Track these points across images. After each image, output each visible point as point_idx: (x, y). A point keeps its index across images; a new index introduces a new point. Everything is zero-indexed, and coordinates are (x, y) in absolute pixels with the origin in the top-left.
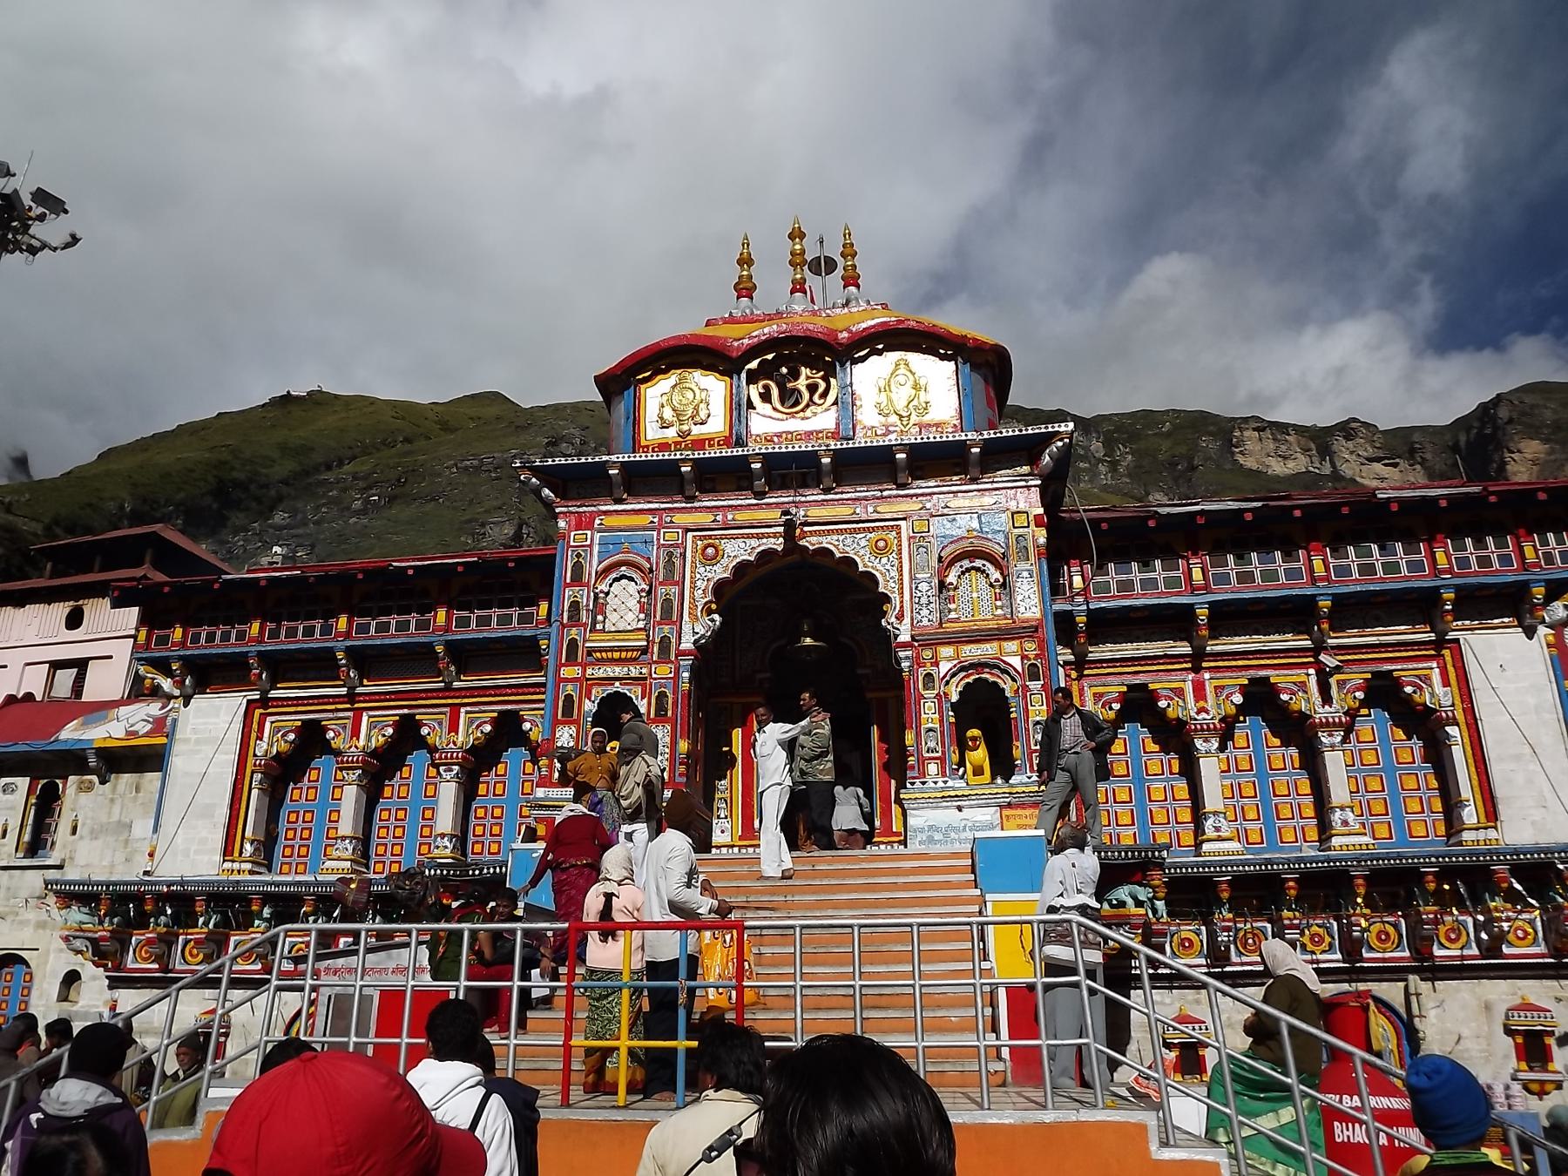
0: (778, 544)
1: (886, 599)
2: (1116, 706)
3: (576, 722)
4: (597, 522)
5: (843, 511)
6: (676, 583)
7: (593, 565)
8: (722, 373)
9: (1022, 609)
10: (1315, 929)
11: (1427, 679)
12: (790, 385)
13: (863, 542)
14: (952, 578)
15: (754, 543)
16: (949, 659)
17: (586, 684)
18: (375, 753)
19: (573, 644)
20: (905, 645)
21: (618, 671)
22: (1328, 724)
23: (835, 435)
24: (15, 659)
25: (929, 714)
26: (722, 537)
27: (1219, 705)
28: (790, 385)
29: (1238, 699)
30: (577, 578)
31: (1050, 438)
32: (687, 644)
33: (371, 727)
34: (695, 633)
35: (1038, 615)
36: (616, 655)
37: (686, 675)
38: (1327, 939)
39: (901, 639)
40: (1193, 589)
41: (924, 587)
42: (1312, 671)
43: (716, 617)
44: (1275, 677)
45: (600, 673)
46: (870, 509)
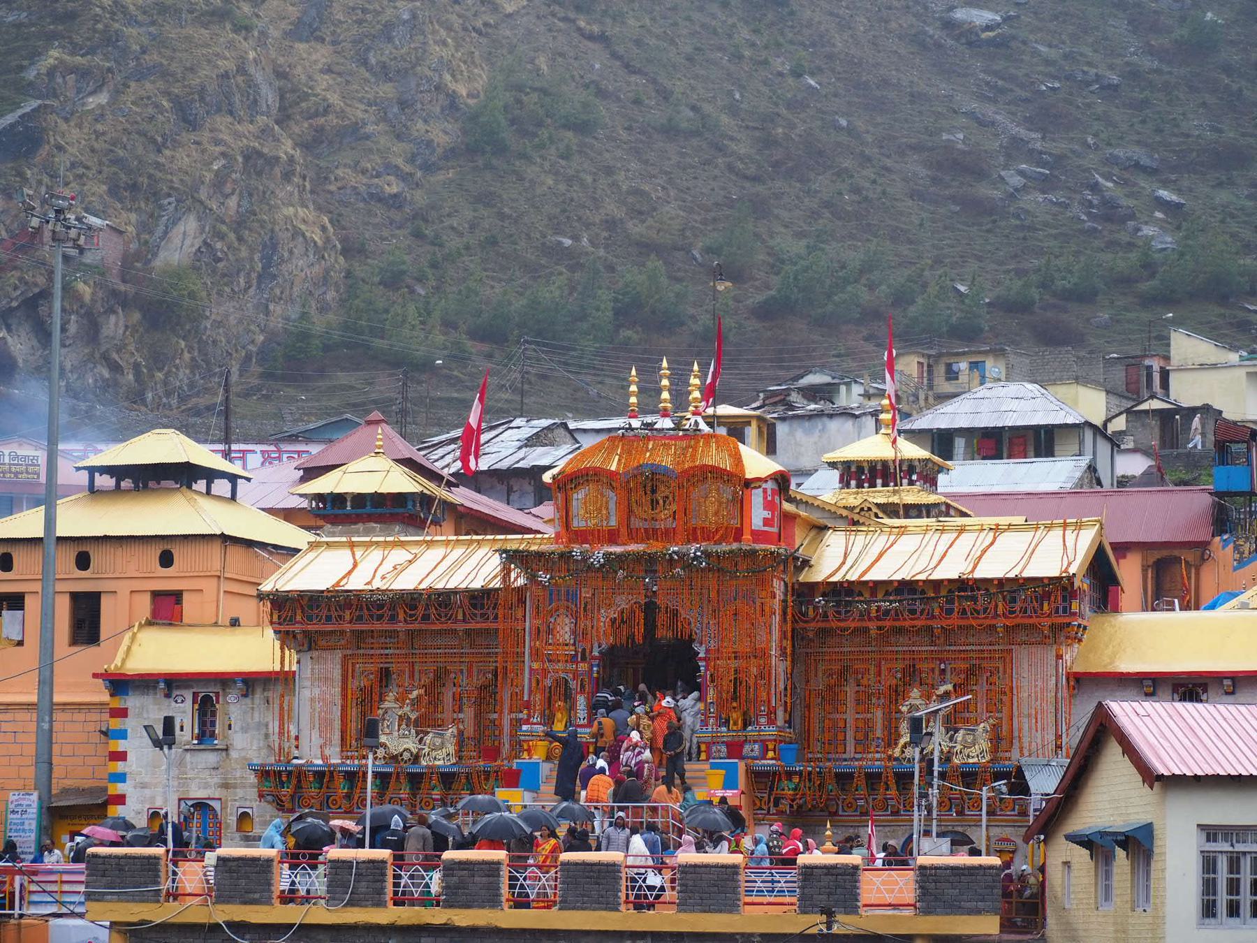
17: (545, 672)
20: (701, 659)
24: (124, 588)
32: (596, 653)
40: (870, 619)
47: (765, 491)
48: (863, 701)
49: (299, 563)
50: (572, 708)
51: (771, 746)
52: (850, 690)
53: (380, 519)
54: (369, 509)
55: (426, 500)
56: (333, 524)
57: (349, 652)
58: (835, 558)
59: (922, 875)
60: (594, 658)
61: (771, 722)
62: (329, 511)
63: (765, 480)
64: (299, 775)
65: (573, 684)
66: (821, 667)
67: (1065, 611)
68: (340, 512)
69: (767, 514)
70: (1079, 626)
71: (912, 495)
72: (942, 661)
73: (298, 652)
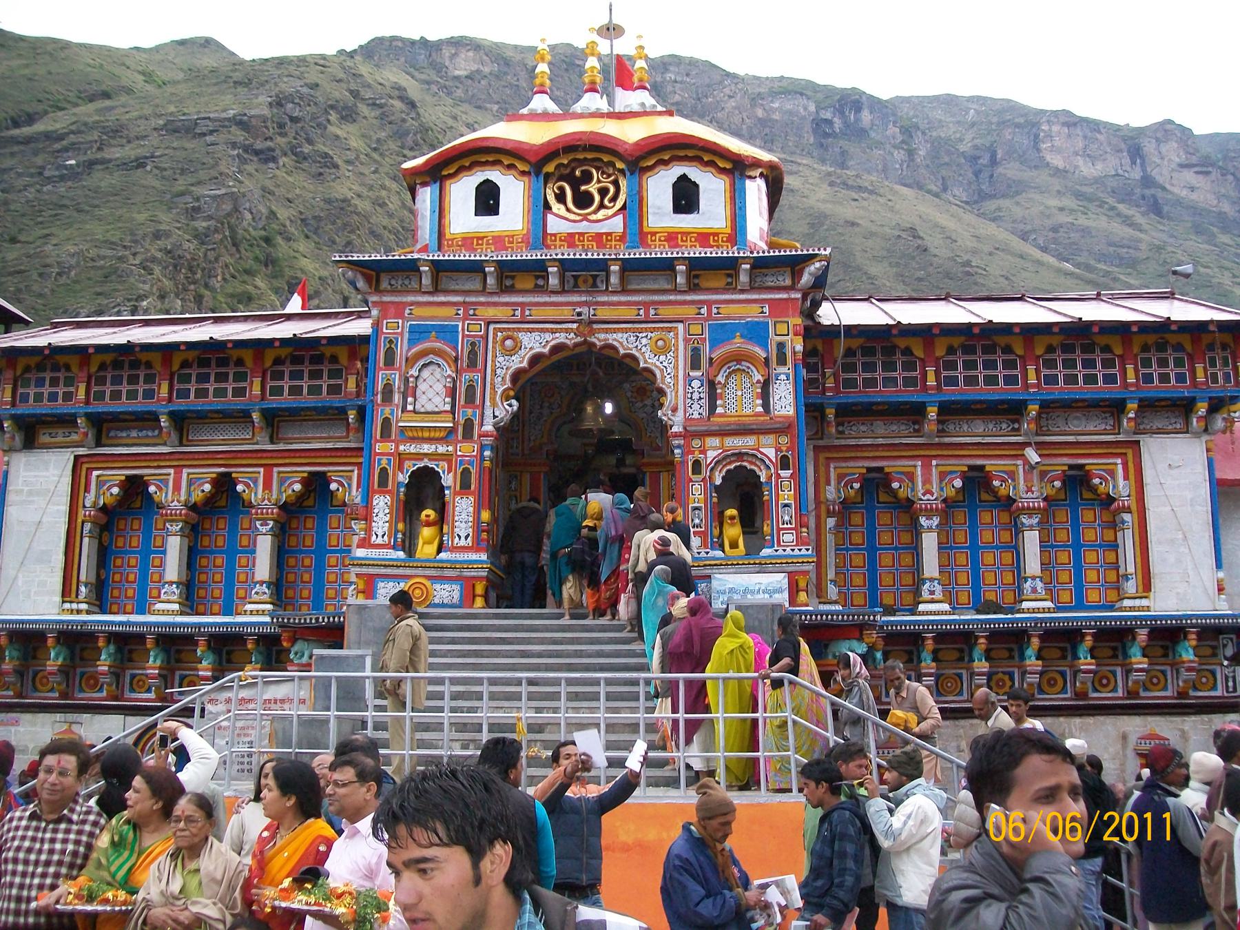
0: (568, 339)
1: (662, 392)
2: (857, 486)
3: (389, 492)
4: (407, 311)
5: (629, 313)
6: (479, 371)
7: (402, 349)
8: (523, 173)
9: (778, 407)
10: (1000, 675)
11: (1112, 473)
12: (583, 188)
13: (644, 341)
14: (720, 378)
15: (548, 336)
16: (715, 448)
17: (401, 458)
18: (193, 508)
19: (386, 421)
20: (676, 435)
21: (427, 448)
22: (1029, 508)
23: (622, 238)
25: (697, 494)
26: (519, 330)
27: (942, 489)
28: (583, 188)
29: (958, 483)
30: (390, 361)
31: (811, 258)
32: (488, 427)
33: (190, 483)
34: (495, 417)
35: (791, 413)
36: (426, 435)
37: (487, 453)
38: (1009, 683)
41: (696, 384)
42: (1020, 462)
43: (514, 402)
44: (991, 465)
45: (412, 448)
46: (652, 312)
50: (441, 520)
51: (802, 584)
57: (82, 451)
60: (486, 435)
61: (800, 541)
65: (448, 480)
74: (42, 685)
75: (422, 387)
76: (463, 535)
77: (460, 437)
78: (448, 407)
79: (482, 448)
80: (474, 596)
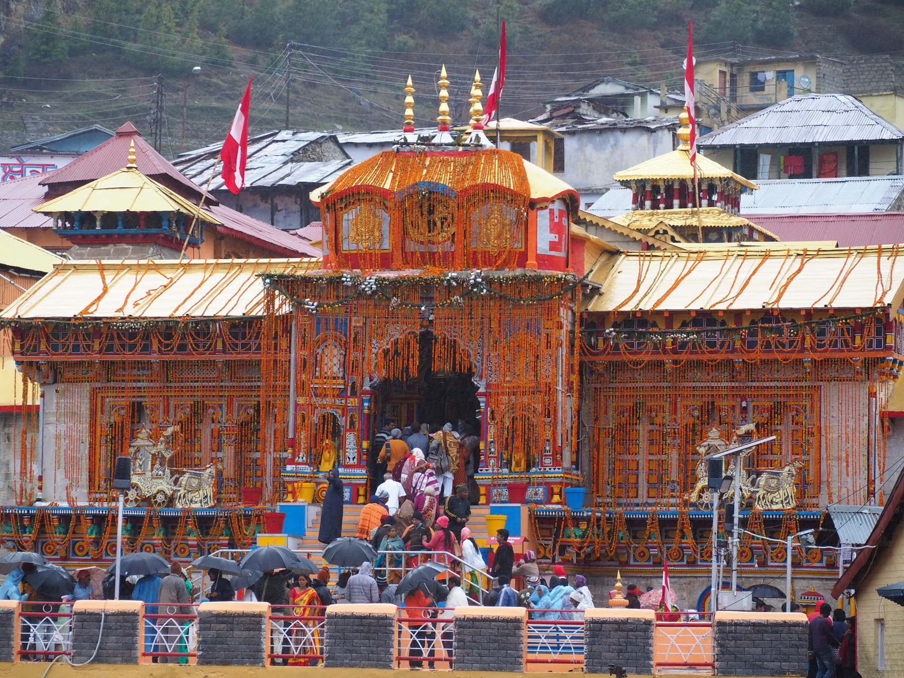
20: (482, 394)
32: (367, 388)
37: (366, 404)
39: (481, 390)
40: (665, 352)
47: (552, 212)
48: (657, 441)
49: (43, 287)
52: (643, 429)
53: (133, 240)
54: (120, 229)
55: (182, 219)
56: (79, 244)
57: (99, 385)
58: (628, 286)
59: (720, 632)
60: (366, 392)
62: (77, 231)
63: (552, 200)
64: (42, 520)
65: (342, 421)
66: (612, 405)
67: (879, 345)
68: (91, 231)
69: (554, 237)
70: (895, 361)
71: (712, 216)
72: (743, 398)
73: (43, 384)
74: (80, 551)
75: (326, 360)
76: (351, 457)
77: (349, 394)
78: (341, 375)
79: (362, 402)
80: (358, 495)
